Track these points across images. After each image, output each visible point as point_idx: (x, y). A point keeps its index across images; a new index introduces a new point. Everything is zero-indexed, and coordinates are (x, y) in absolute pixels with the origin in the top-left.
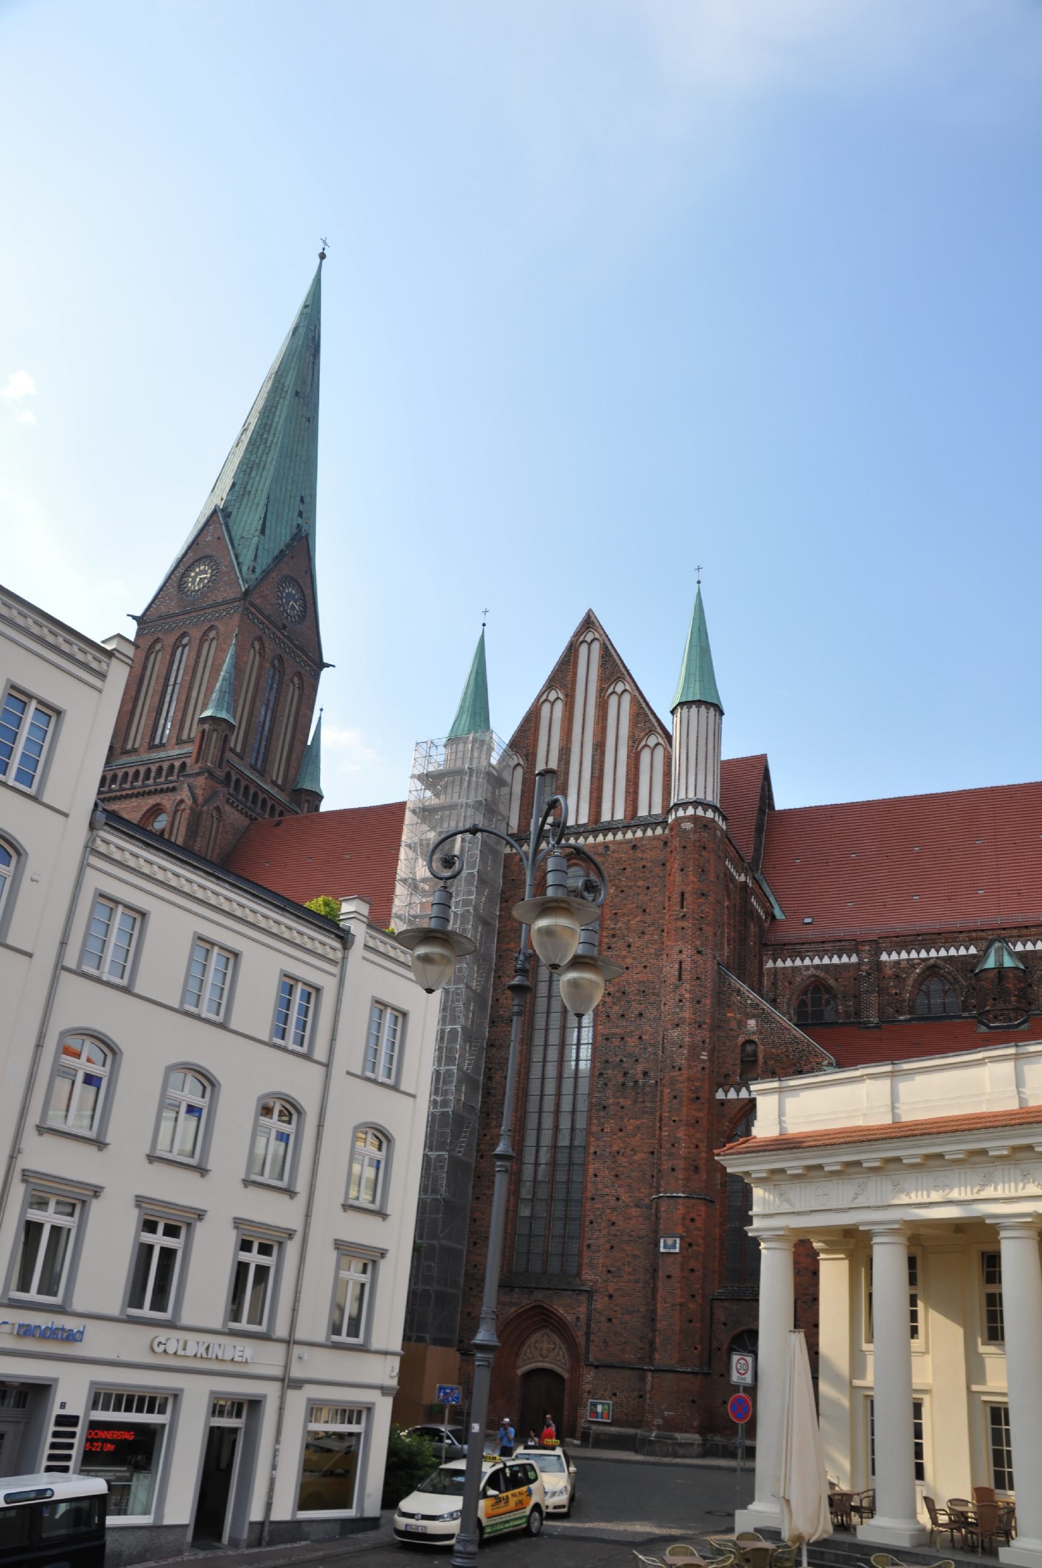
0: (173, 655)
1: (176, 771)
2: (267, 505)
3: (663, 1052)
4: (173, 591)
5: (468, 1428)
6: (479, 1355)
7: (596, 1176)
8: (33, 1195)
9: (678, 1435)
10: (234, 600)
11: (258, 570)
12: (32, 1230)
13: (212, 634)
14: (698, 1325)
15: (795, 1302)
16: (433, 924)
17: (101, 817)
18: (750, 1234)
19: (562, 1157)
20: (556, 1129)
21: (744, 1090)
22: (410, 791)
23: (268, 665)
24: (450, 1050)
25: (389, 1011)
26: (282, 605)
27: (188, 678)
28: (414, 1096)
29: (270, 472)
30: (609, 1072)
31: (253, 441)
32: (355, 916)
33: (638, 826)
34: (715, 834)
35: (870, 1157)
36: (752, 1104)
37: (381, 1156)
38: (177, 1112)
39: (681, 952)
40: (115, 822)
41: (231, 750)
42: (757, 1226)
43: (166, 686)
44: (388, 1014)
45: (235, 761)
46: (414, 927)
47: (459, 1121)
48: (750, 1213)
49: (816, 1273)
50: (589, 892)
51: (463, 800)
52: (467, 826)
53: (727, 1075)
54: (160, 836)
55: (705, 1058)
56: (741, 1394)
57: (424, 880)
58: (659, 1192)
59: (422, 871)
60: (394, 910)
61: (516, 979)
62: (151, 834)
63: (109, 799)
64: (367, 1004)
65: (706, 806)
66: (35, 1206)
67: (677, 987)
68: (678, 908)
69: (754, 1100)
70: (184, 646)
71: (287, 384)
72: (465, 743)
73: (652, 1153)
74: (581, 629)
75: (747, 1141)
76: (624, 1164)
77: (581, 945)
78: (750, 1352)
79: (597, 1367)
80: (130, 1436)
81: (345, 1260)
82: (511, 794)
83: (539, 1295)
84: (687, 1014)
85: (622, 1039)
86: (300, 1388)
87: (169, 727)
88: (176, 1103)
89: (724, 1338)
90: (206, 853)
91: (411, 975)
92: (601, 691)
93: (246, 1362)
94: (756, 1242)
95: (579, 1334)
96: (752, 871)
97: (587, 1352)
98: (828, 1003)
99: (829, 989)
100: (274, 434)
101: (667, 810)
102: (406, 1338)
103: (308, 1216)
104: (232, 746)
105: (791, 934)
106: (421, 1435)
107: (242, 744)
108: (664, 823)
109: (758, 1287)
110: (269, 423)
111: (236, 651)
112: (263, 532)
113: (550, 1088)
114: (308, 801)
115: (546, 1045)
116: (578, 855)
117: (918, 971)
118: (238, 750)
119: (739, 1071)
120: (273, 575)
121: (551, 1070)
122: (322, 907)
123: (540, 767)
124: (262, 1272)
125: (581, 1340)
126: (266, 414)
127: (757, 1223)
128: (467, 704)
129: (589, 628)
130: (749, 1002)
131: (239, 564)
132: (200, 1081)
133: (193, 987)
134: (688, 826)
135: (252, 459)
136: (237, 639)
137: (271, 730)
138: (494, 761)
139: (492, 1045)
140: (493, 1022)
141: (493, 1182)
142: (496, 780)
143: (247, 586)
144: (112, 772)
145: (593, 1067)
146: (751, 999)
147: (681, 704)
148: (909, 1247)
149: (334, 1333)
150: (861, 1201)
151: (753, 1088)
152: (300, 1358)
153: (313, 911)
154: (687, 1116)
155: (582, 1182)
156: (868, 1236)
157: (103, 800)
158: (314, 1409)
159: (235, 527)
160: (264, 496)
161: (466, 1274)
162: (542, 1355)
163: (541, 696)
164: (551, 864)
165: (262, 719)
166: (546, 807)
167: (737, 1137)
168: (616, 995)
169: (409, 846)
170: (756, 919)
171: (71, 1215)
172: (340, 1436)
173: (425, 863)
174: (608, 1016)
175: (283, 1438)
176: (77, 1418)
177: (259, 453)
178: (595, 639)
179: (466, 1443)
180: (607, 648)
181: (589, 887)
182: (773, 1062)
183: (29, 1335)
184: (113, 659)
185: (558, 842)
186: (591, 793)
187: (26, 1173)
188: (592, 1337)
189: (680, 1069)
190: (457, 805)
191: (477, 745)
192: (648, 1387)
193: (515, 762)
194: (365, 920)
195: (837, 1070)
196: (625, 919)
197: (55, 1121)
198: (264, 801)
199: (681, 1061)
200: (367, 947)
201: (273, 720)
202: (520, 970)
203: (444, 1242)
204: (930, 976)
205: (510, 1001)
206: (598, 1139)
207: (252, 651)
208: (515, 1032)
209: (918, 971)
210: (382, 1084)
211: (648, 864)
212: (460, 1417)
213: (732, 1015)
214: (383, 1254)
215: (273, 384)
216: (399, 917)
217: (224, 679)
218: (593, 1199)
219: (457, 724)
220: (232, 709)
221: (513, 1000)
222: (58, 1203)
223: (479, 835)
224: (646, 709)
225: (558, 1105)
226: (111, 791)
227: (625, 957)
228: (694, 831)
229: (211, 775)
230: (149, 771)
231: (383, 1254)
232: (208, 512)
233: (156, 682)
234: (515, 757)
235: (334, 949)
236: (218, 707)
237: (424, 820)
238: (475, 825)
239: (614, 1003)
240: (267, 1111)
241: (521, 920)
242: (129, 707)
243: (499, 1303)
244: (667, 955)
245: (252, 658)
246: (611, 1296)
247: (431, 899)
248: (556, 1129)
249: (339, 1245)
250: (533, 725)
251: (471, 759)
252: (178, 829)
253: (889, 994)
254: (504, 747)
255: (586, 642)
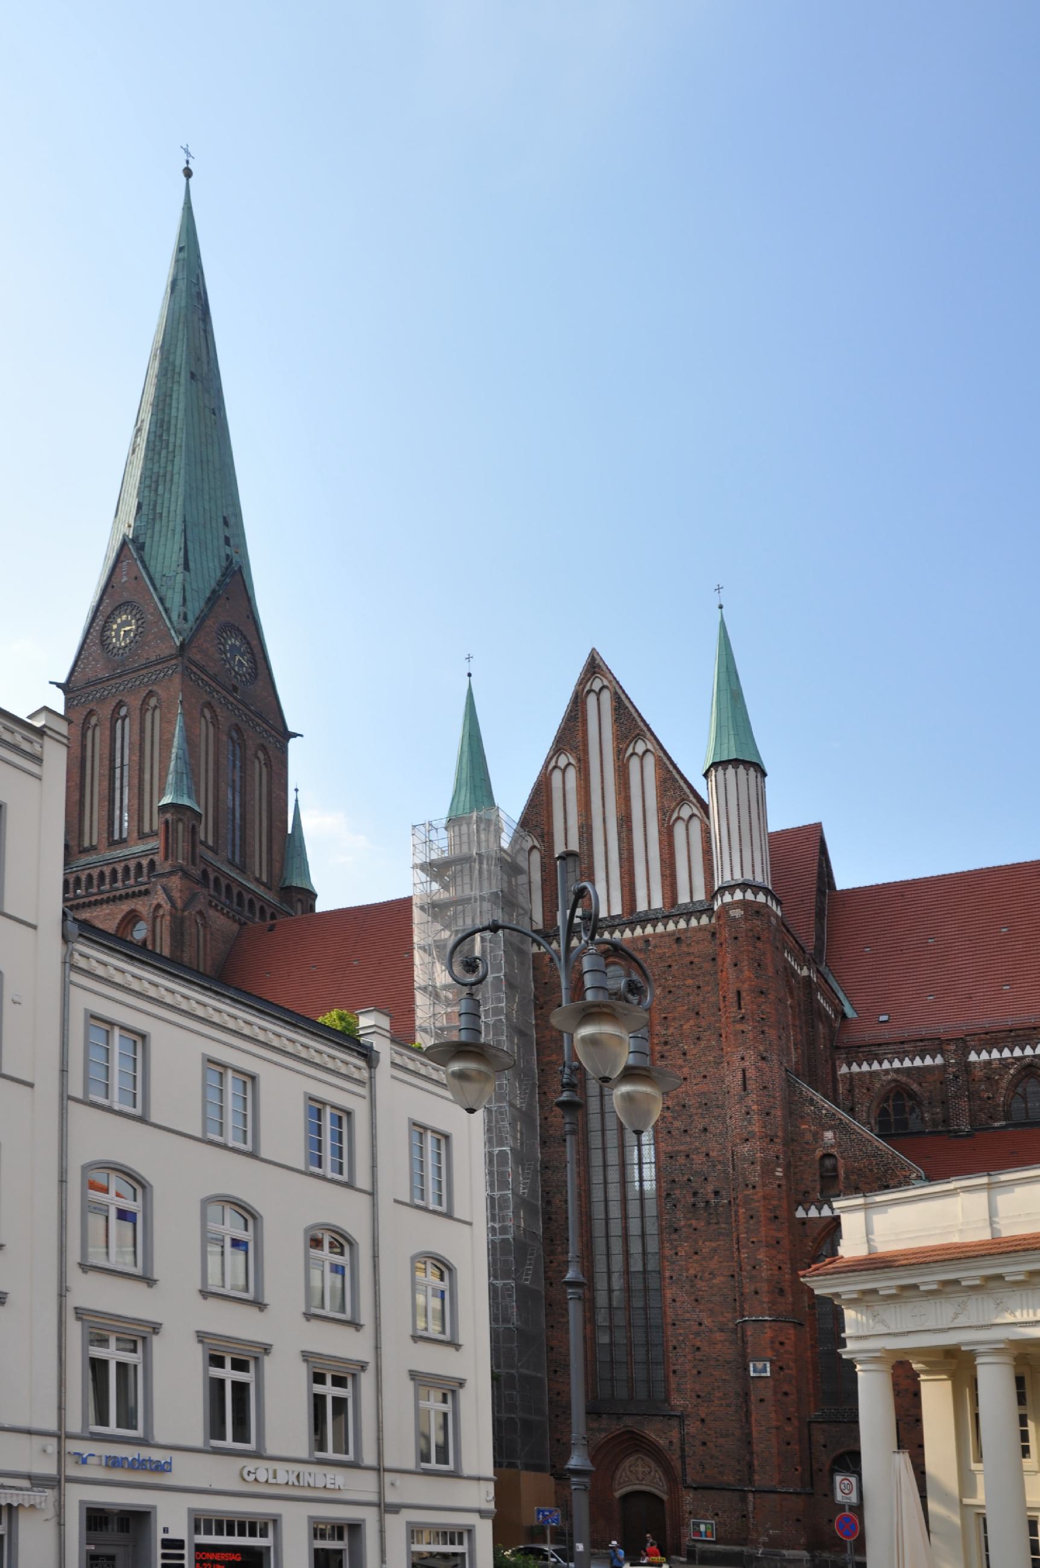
0: (113, 729)
1: (145, 870)
2: (185, 531)
3: (734, 1170)
4: (96, 649)
5: (572, 1548)
6: (574, 1479)
7: (674, 1301)
8: (91, 1333)
9: (785, 1552)
10: (171, 657)
11: (191, 617)
12: (98, 1367)
13: (153, 702)
14: (797, 1447)
15: (897, 1424)
16: (464, 1037)
17: (73, 928)
18: (844, 1357)
19: (637, 1284)
20: (627, 1254)
21: (826, 1207)
22: (415, 884)
24: (502, 1175)
25: (429, 1134)
26: (227, 661)
27: (136, 758)
28: (470, 1224)
29: (179, 487)
30: (677, 1192)
31: (151, 445)
32: (376, 1030)
33: (680, 915)
34: (769, 921)
35: (971, 1275)
36: (836, 1222)
37: (444, 1285)
38: (223, 1247)
39: (743, 1059)
40: (90, 932)
41: (202, 843)
42: (851, 1348)
43: (112, 769)
44: (430, 1139)
45: (209, 855)
46: (442, 1041)
47: (521, 1248)
48: (843, 1335)
49: (917, 1394)
50: (633, 994)
51: (476, 893)
52: (486, 923)
53: (806, 1193)
54: (142, 947)
55: (781, 1174)
56: (847, 1513)
57: (446, 987)
58: (743, 1316)
59: (442, 977)
60: (418, 1022)
61: (565, 1094)
62: (131, 944)
63: (77, 907)
64: (404, 1128)
65: (757, 889)
66: (96, 1343)
67: (742, 1098)
68: (735, 1009)
69: (839, 1217)
70: (124, 718)
71: (177, 363)
72: (468, 824)
73: (733, 1276)
74: (585, 675)
75: (834, 1261)
76: (703, 1289)
77: (631, 1055)
78: (853, 1472)
79: (695, 1489)
80: (238, 1558)
81: (423, 1391)
82: (530, 882)
83: (629, 1421)
84: (756, 1128)
85: (688, 1156)
86: (397, 1512)
87: (126, 818)
88: (220, 1237)
89: (825, 1460)
90: (198, 965)
91: (448, 1094)
92: (619, 752)
93: (339, 1489)
94: (851, 1364)
95: (674, 1457)
96: (815, 963)
97: (684, 1475)
98: (912, 1110)
99: (912, 1095)
100: (175, 435)
101: (712, 895)
102: (497, 1464)
103: (377, 1348)
104: (203, 838)
105: (867, 1035)
106: (526, 1554)
107: (214, 836)
108: (709, 911)
109: (857, 1409)
110: (166, 419)
111: (185, 722)
113: (615, 1211)
114: (300, 900)
115: (605, 1166)
116: (615, 951)
117: (1012, 1071)
118: (210, 842)
119: (818, 1187)
120: (209, 622)
121: (614, 1193)
122: (337, 1022)
123: (559, 849)
124: (340, 1404)
125: (677, 1463)
126: (160, 407)
127: (850, 1345)
128: (464, 776)
129: (594, 673)
130: (824, 1112)
131: (166, 610)
132: (242, 1216)
133: (213, 1113)
134: (737, 913)
135: (156, 470)
136: (183, 708)
137: (243, 817)
138: (505, 843)
139: (547, 1168)
140: (543, 1143)
141: (567, 1310)
142: (510, 867)
143: (181, 638)
144: (74, 875)
145: (659, 1188)
146: (826, 1109)
147: (715, 765)
148: (1015, 1367)
149: (423, 1461)
150: (962, 1321)
151: (835, 1205)
152: (392, 1484)
153: (328, 1027)
154: (767, 1237)
155: (661, 1308)
156: (971, 1356)
157: (71, 908)
158: (414, 1532)
159: (153, 563)
160: (179, 519)
161: (550, 1402)
162: (637, 1478)
163: (549, 762)
164: (586, 963)
165: (230, 804)
166: (572, 898)
167: (822, 1257)
168: (676, 1109)
169: (423, 948)
170: (824, 1018)
171: (134, 1351)
172: (445, 1556)
173: (444, 968)
174: (669, 1132)
175: (388, 1558)
176: (182, 1541)
178: (604, 687)
179: (572, 1561)
180: (619, 698)
181: (633, 988)
182: (855, 1177)
183: (118, 1466)
184: (46, 738)
185: (592, 938)
186: (622, 878)
187: (79, 1311)
188: (688, 1460)
189: (754, 1187)
190: (470, 899)
191: (482, 826)
192: (751, 1508)
193: (530, 844)
194: (388, 1035)
195: (927, 1183)
196: (676, 1024)
197: (97, 1258)
198: (251, 902)
199: (755, 1179)
200: (394, 1064)
201: (243, 805)
202: (568, 1084)
203: (524, 1371)
204: (1026, 1076)
205: (560, 1119)
206: (673, 1263)
207: (203, 720)
208: (570, 1152)
209: (1012, 1071)
210: (434, 1212)
211: (696, 960)
212: (564, 1538)
213: (807, 1126)
214: (461, 1383)
215: (161, 364)
216: (425, 1030)
217: (177, 757)
218: (674, 1324)
219: (456, 800)
220: (193, 793)
221: (563, 1117)
222: (118, 1339)
223: (500, 932)
224: (674, 772)
225: (625, 1229)
226: (77, 897)
227: (681, 1067)
228: (745, 918)
229: (186, 874)
230: (114, 872)
231: (461, 1383)
232: (117, 545)
233: (101, 765)
234: (529, 839)
235: (359, 1068)
236: (178, 791)
237: (435, 917)
238: (494, 921)
239: (675, 1118)
240: (316, 1243)
241: (560, 1029)
242: (76, 796)
243: (588, 1429)
244: (728, 1064)
245: (204, 729)
246: (703, 1421)
247: (456, 1009)
248: (627, 1254)
249: (414, 1375)
250: (544, 798)
251: (479, 843)
252: (161, 938)
253: (981, 1099)
254: (515, 826)
255: (594, 691)
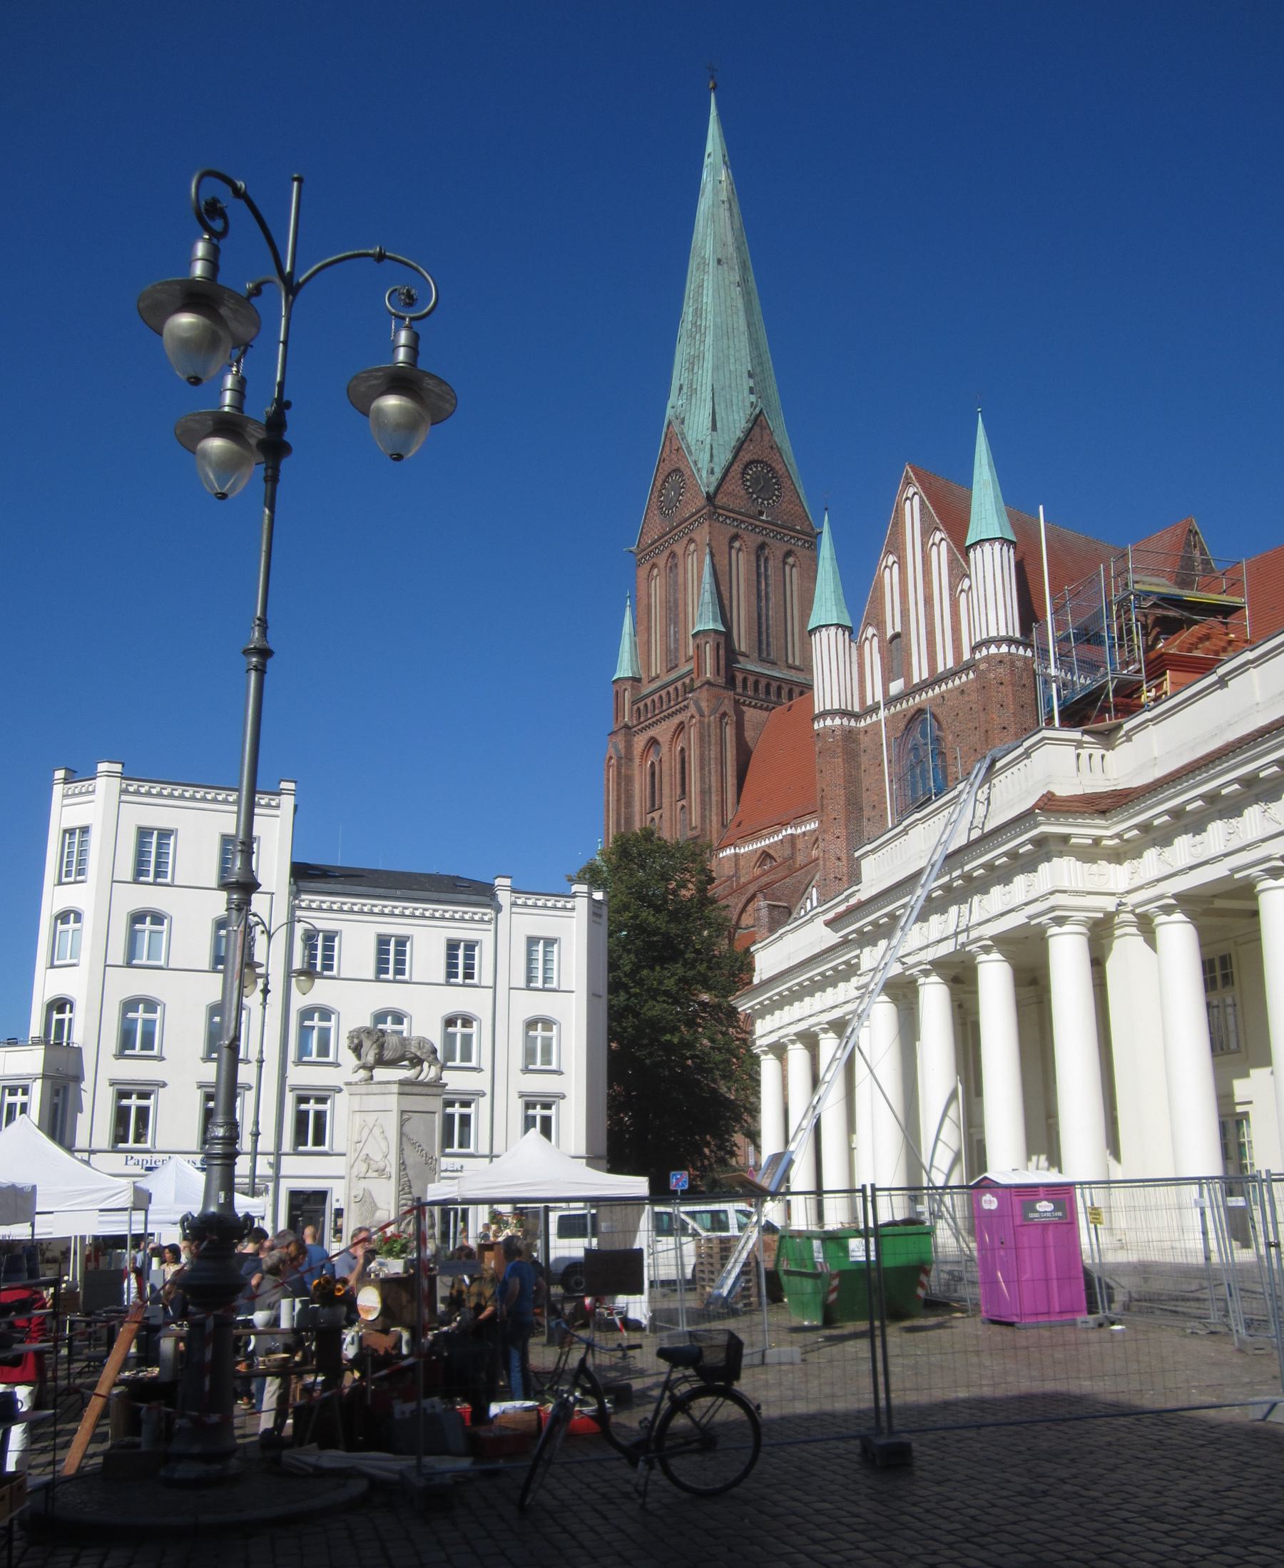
112: (714, 428)
131: (698, 470)
160: (709, 389)
177: (697, 343)
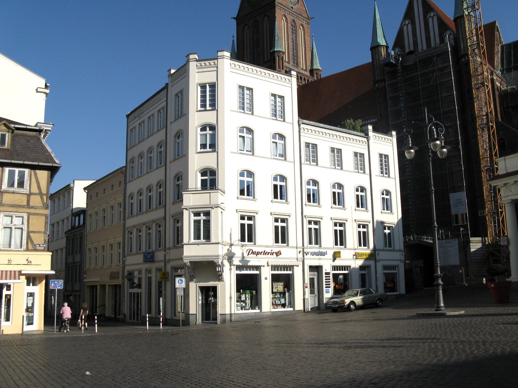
23: (289, 25)
